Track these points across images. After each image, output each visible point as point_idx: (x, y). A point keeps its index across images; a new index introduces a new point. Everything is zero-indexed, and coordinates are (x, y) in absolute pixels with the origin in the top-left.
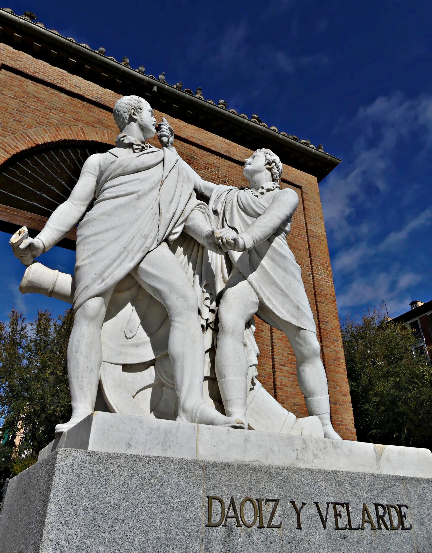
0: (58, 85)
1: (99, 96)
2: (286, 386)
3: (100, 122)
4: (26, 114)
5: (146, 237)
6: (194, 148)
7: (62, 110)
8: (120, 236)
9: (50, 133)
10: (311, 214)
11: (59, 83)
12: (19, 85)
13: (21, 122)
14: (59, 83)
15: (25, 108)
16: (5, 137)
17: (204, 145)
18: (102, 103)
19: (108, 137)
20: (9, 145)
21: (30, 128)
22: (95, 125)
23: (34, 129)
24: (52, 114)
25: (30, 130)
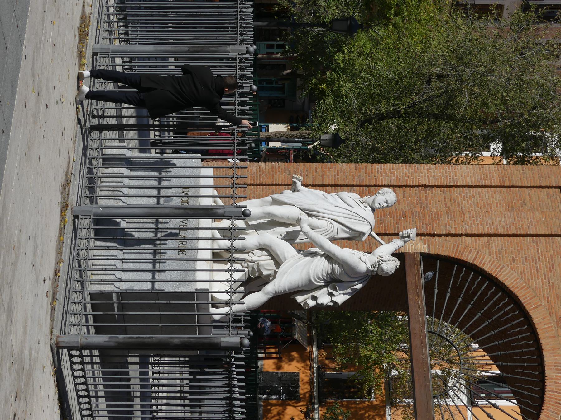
4: (525, 263)
9: (517, 283)
12: (557, 252)
13: (514, 261)
15: (533, 261)
19: (546, 328)
21: (511, 268)
22: (554, 316)
23: (512, 272)
24: (540, 280)
25: (508, 269)
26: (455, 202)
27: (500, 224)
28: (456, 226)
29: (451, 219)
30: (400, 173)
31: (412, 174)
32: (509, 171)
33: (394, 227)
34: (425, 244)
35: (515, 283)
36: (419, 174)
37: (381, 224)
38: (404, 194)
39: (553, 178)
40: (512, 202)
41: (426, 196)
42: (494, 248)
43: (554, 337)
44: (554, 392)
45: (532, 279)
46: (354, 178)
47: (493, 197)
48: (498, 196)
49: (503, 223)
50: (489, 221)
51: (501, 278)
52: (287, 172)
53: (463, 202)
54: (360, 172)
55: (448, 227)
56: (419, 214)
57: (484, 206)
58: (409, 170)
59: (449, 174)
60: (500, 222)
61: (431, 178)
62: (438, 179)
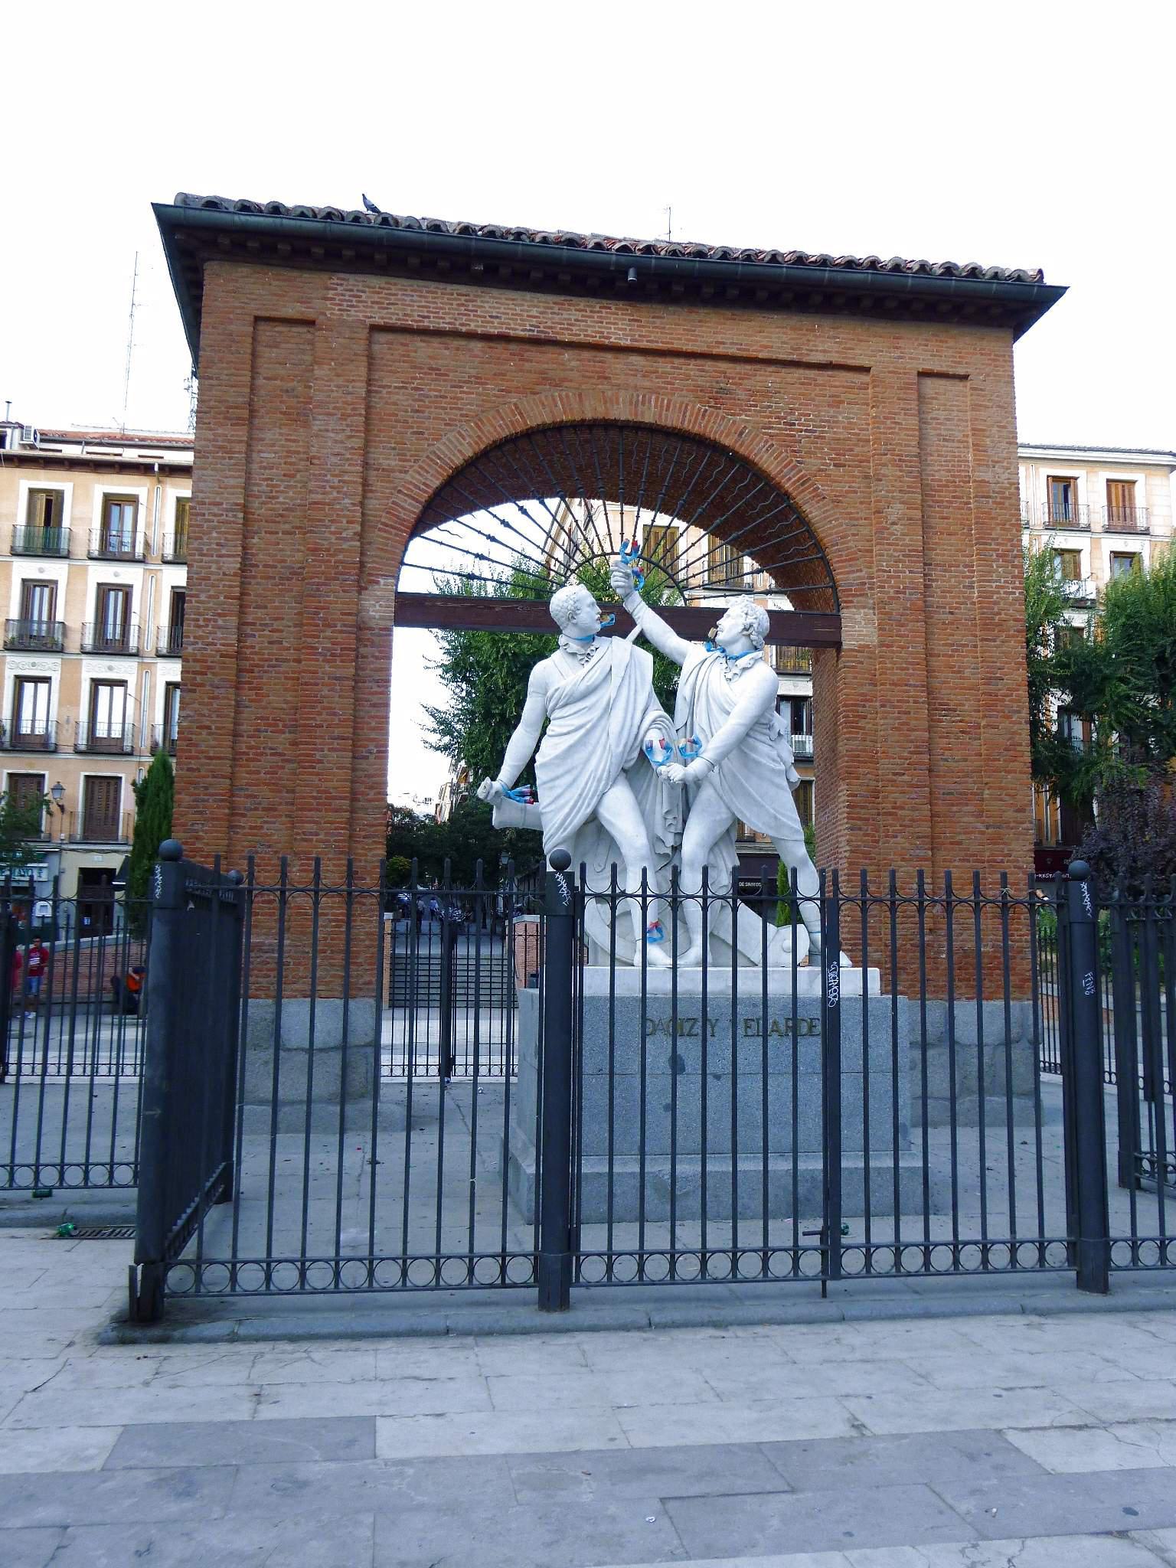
0: (464, 329)
1: (534, 321)
2: (902, 808)
3: (545, 379)
5: (599, 781)
6: (723, 366)
7: (479, 380)
8: (574, 780)
10: (988, 441)
11: (462, 325)
13: (422, 433)
14: (462, 325)
16: (406, 472)
17: (745, 354)
18: (543, 336)
20: (416, 486)
21: (437, 440)
22: (539, 388)
23: (444, 440)
25: (438, 445)
26: (282, 516)
27: (342, 442)
28: (344, 521)
29: (327, 527)
30: (209, 609)
31: (213, 586)
32: (212, 403)
33: (341, 632)
34: (378, 583)
35: (468, 440)
36: (212, 573)
37: (333, 655)
38: (258, 607)
39: (232, 327)
40: (284, 413)
41: (265, 566)
42: (393, 463)
43: (580, 395)
44: (684, 416)
45: (460, 409)
46: (217, 698)
47: (273, 445)
48: (268, 436)
49: (340, 437)
50: (334, 459)
51: (458, 461)
52: (196, 827)
53: (281, 500)
54: (202, 685)
55: (344, 535)
56: (313, 584)
57: (291, 464)
58: (202, 591)
59: (215, 515)
60: (336, 442)
61: (224, 552)
62: (226, 539)
